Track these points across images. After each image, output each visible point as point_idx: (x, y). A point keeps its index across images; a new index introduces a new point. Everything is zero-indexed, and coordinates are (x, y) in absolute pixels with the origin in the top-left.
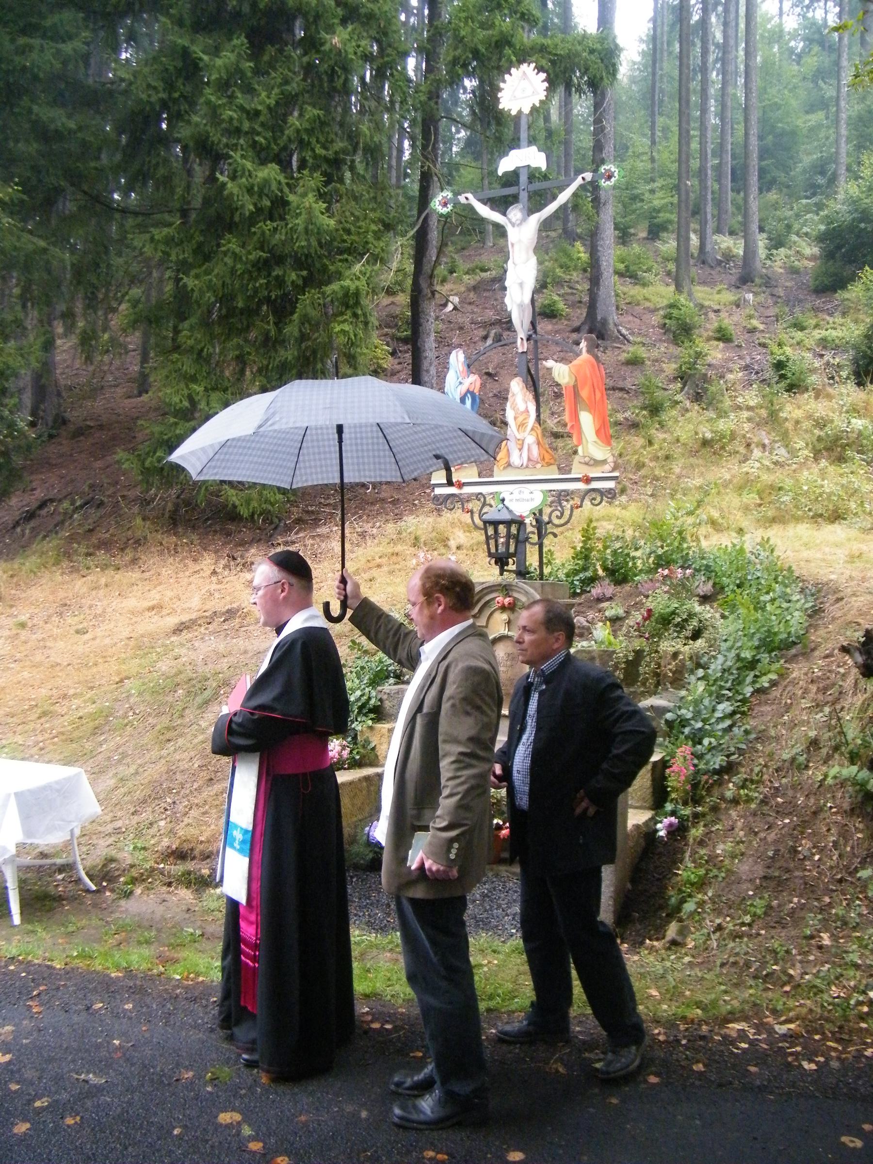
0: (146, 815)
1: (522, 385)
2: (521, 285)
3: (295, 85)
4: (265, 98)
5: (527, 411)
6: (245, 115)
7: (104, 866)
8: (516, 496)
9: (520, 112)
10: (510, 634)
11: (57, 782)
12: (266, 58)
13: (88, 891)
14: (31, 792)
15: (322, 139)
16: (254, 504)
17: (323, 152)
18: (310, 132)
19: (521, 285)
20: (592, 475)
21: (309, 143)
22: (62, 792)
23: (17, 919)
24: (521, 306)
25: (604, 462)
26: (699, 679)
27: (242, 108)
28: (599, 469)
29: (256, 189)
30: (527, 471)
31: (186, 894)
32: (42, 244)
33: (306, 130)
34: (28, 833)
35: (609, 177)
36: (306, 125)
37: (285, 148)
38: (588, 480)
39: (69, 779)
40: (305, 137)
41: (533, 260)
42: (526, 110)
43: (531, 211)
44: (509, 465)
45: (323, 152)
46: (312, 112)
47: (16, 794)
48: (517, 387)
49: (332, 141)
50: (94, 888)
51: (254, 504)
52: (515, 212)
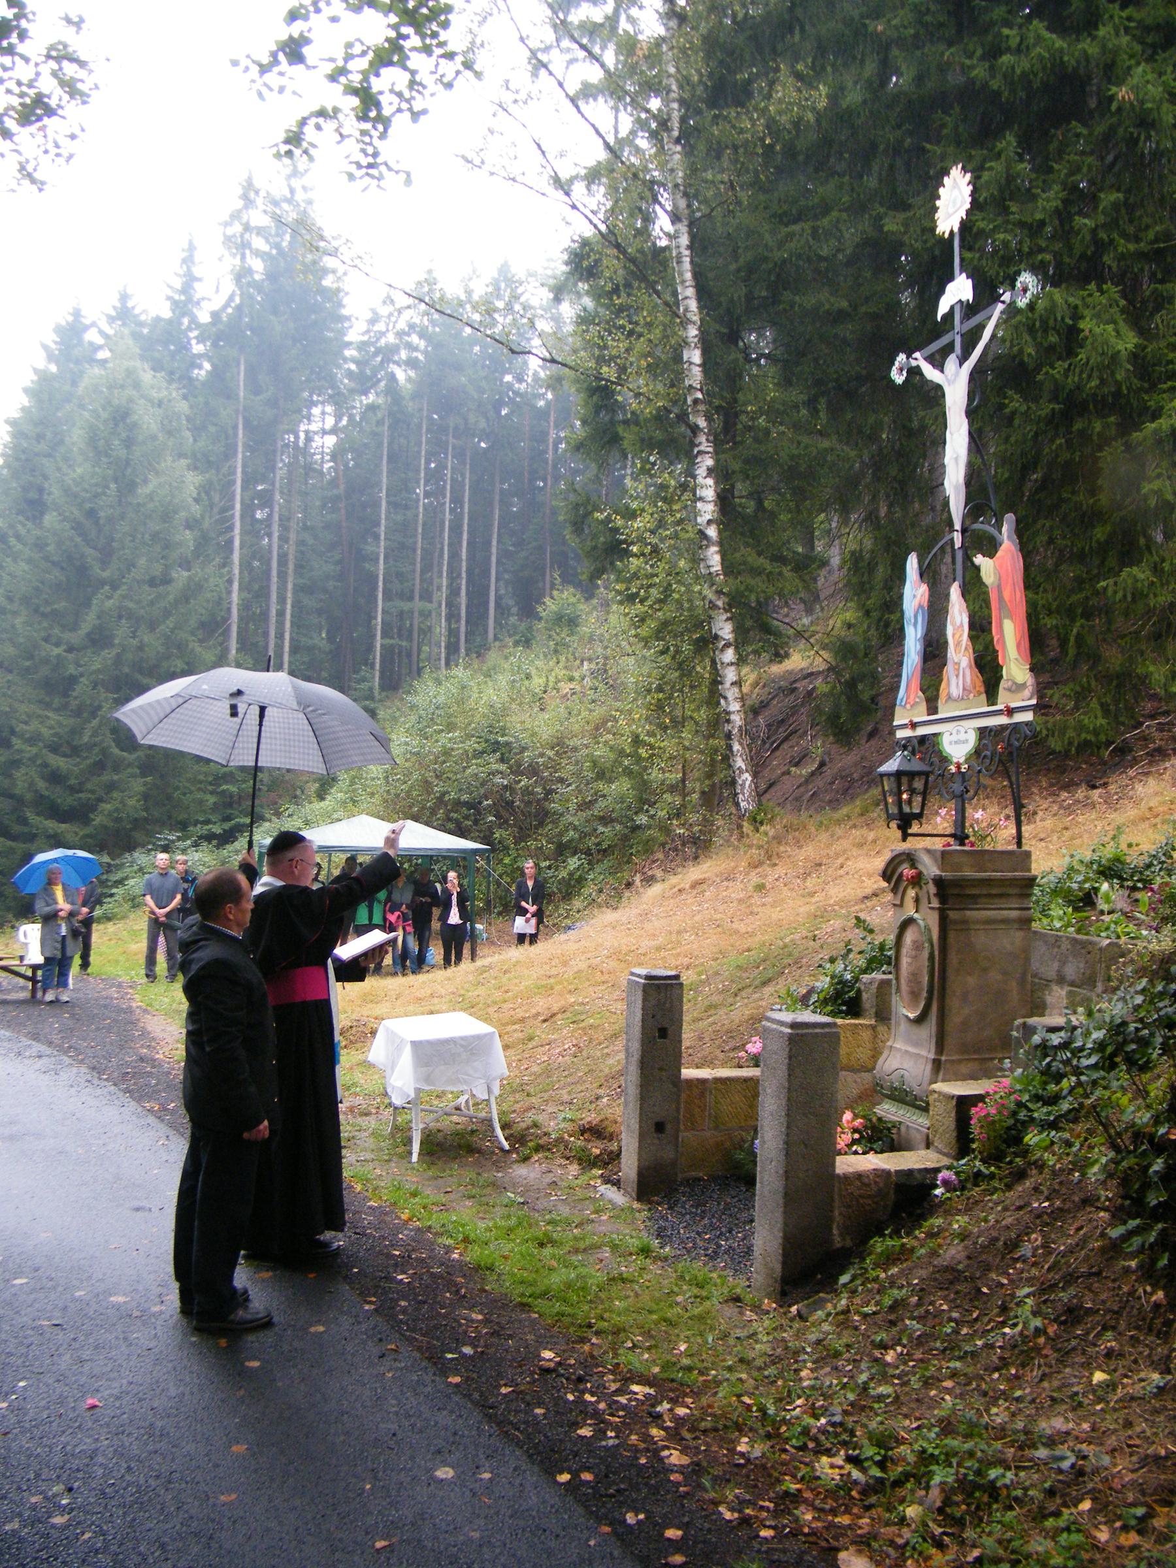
0: (601, 1092)
1: (959, 592)
2: (956, 459)
3: (1085, 170)
4: (1050, 199)
5: (962, 625)
6: (1026, 231)
7: (528, 1128)
8: (954, 738)
9: (952, 232)
10: (916, 916)
11: (462, 1038)
12: (1053, 147)
13: (502, 1149)
14: (430, 1043)
15: (1131, 230)
16: (1071, 733)
17: (1132, 247)
18: (1112, 224)
19: (956, 459)
20: (1013, 705)
21: (1112, 241)
22: (471, 1047)
23: (415, 1158)
24: (956, 487)
25: (1023, 686)
26: (1137, 993)
27: (1021, 224)
28: (1020, 695)
29: (1038, 324)
30: (963, 704)
31: (574, 1169)
32: (826, 444)
33: (1104, 226)
34: (428, 1079)
35: (1025, 290)
36: (1101, 219)
37: (1083, 256)
38: (1010, 712)
39: (478, 1037)
40: (1103, 235)
41: (965, 422)
42: (956, 230)
43: (962, 360)
44: (949, 697)
45: (1132, 247)
46: (1109, 198)
47: (415, 1045)
48: (955, 592)
49: (1147, 227)
50: (506, 1146)
51: (1071, 733)
52: (951, 362)
